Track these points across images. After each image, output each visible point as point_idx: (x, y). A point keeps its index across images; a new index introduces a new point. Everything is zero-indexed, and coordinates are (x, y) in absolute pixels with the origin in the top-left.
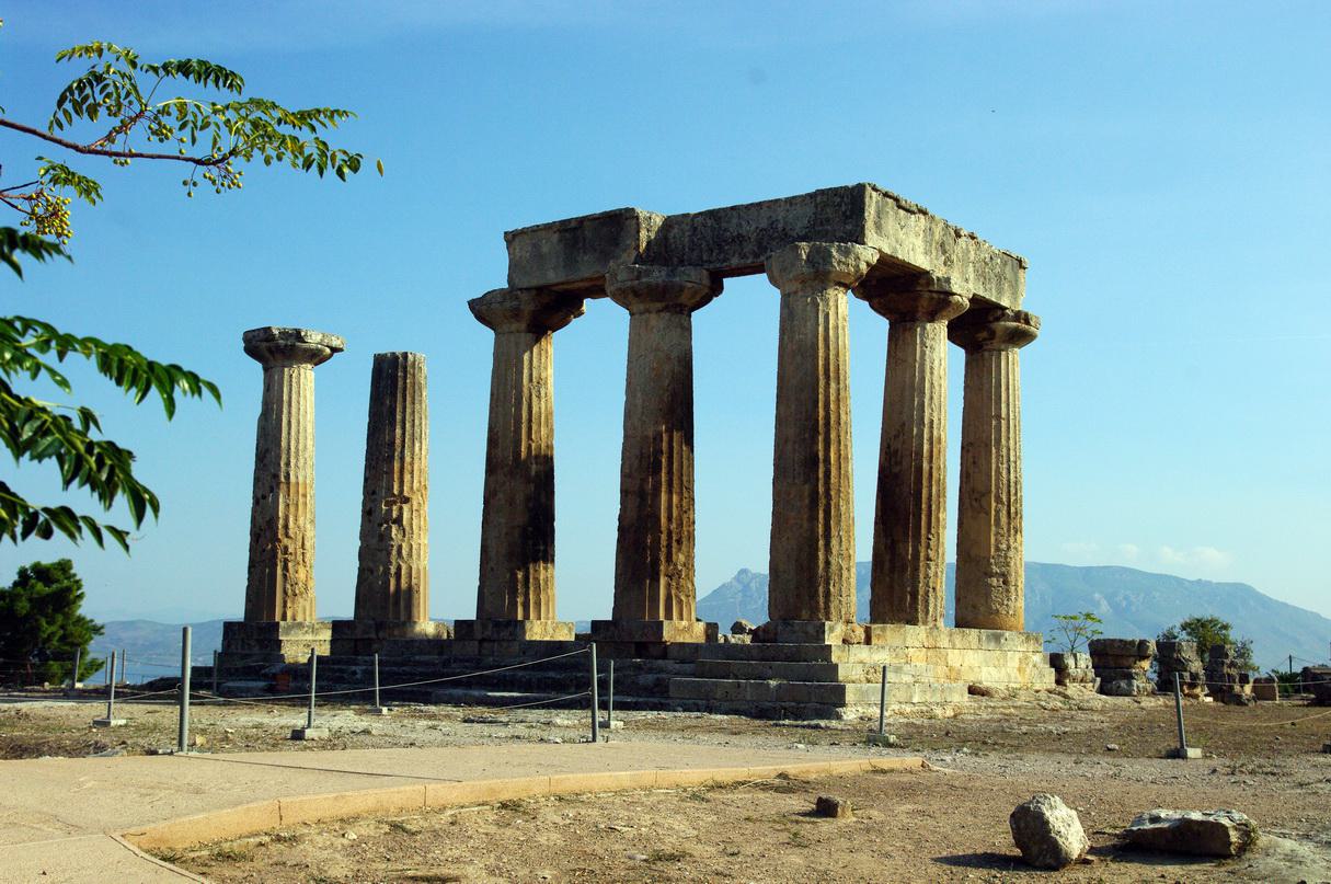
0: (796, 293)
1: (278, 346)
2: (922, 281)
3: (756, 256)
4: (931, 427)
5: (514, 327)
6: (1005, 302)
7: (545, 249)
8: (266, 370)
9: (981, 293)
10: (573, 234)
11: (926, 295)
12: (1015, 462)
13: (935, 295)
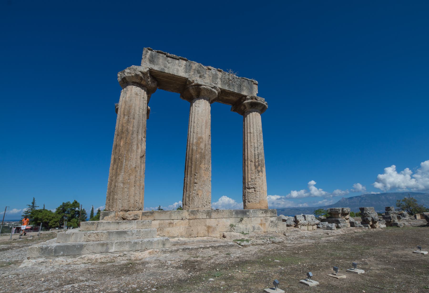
2: (188, 83)
4: (197, 134)
6: (244, 93)
9: (226, 88)
11: (191, 88)
12: (258, 147)
13: (193, 87)
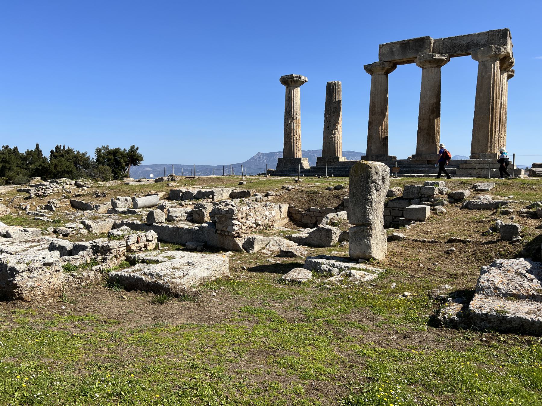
0: (487, 61)
1: (294, 80)
3: (467, 51)
5: (380, 73)
7: (394, 50)
8: (287, 88)
10: (405, 45)
